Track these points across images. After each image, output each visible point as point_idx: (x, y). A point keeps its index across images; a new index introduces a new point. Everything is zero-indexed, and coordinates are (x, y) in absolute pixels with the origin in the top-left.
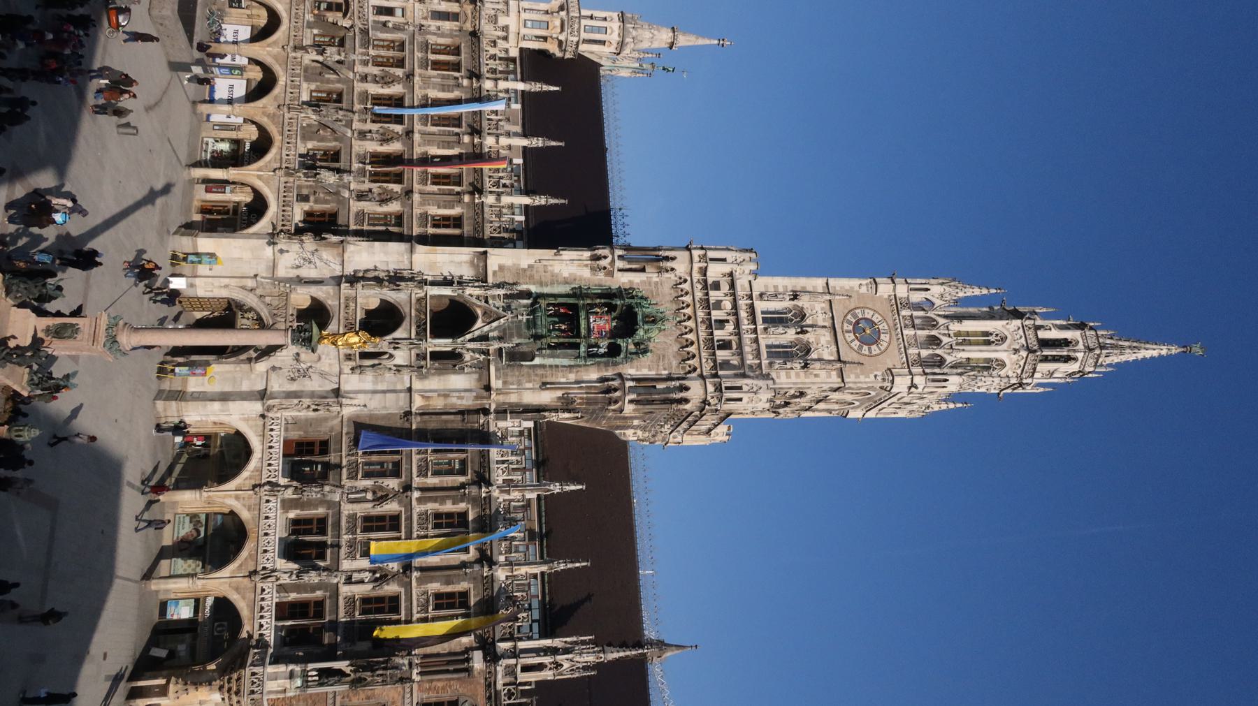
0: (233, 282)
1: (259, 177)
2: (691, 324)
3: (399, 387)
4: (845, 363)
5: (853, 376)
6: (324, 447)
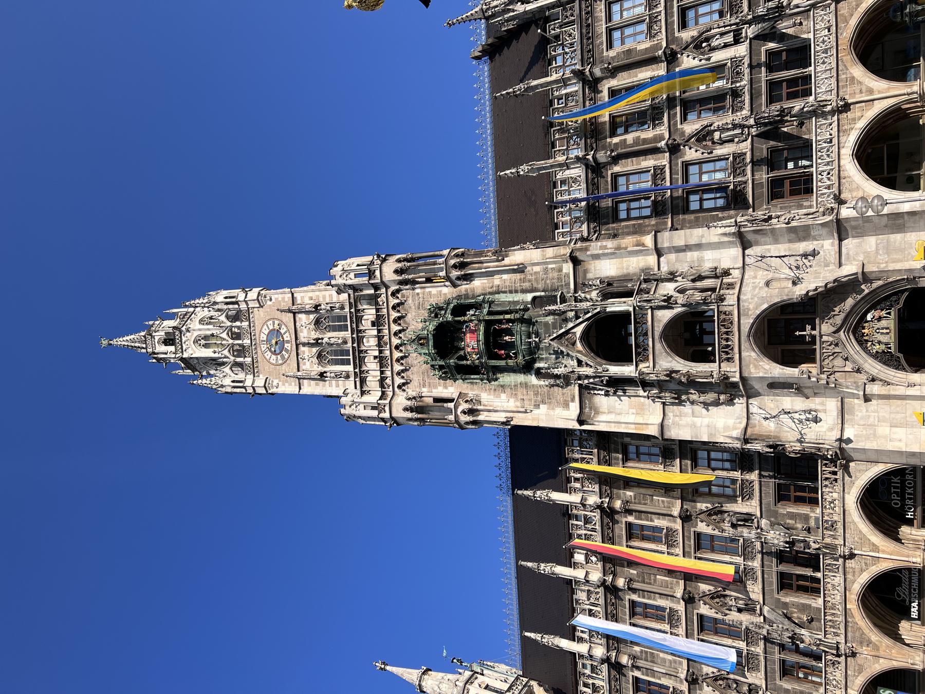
0: (901, 391)
3: (672, 256)
4: (290, 311)
5: (286, 299)
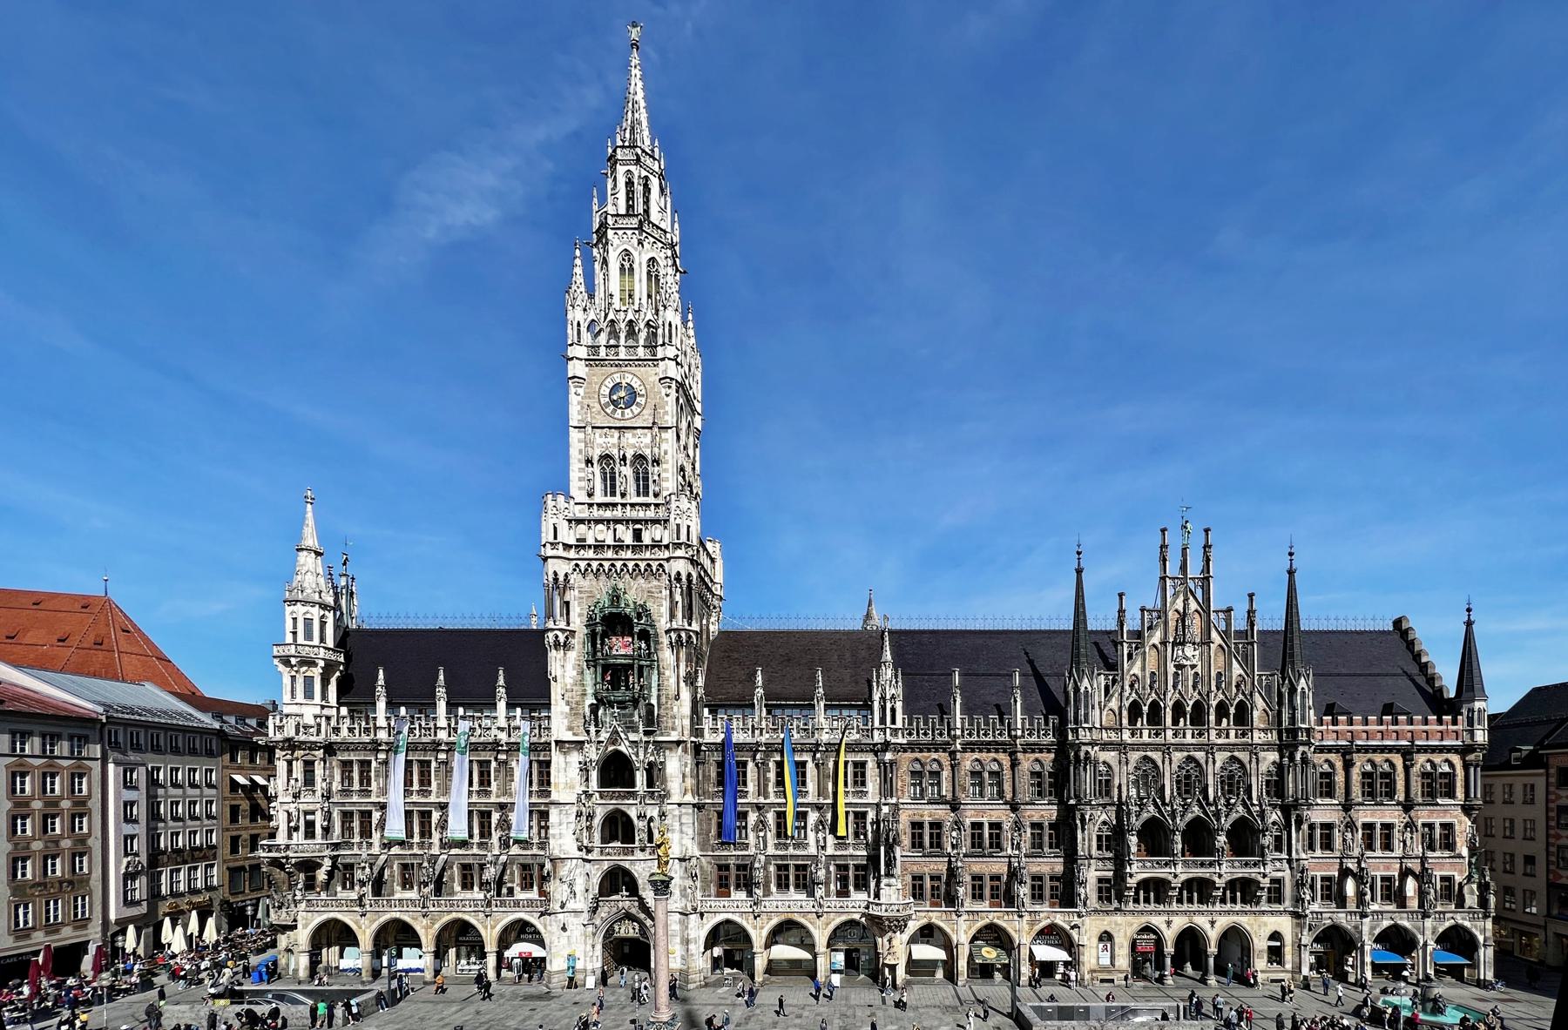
1: (493, 927)
2: (619, 564)
6: (723, 868)
